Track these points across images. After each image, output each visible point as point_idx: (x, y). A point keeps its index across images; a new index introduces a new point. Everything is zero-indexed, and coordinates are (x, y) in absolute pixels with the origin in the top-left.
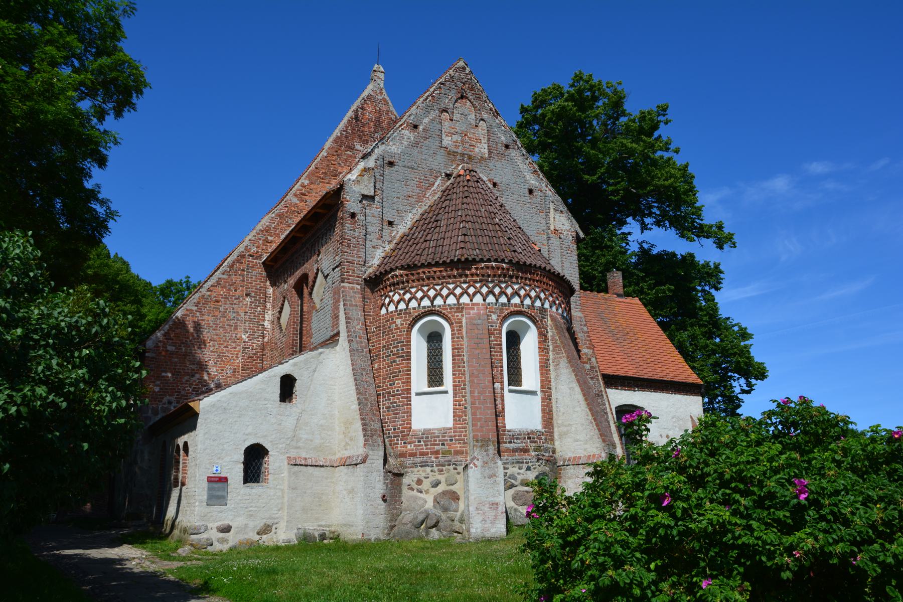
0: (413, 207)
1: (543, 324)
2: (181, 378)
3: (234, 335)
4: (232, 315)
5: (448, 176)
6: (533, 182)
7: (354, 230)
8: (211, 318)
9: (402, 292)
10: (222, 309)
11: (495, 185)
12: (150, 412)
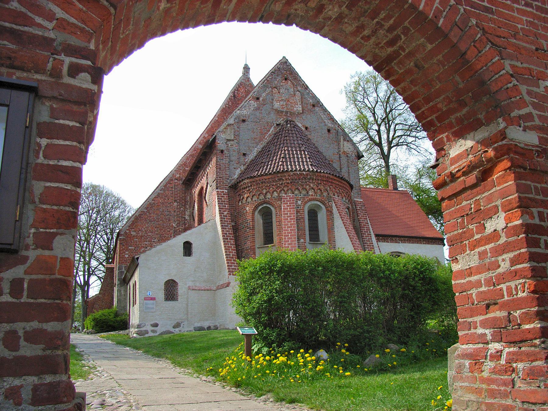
0: (258, 145)
1: (329, 205)
2: (140, 249)
3: (168, 224)
4: (167, 213)
5: (277, 125)
6: (330, 125)
7: (223, 160)
8: (155, 216)
10: (161, 210)
11: (306, 128)
12: (123, 269)
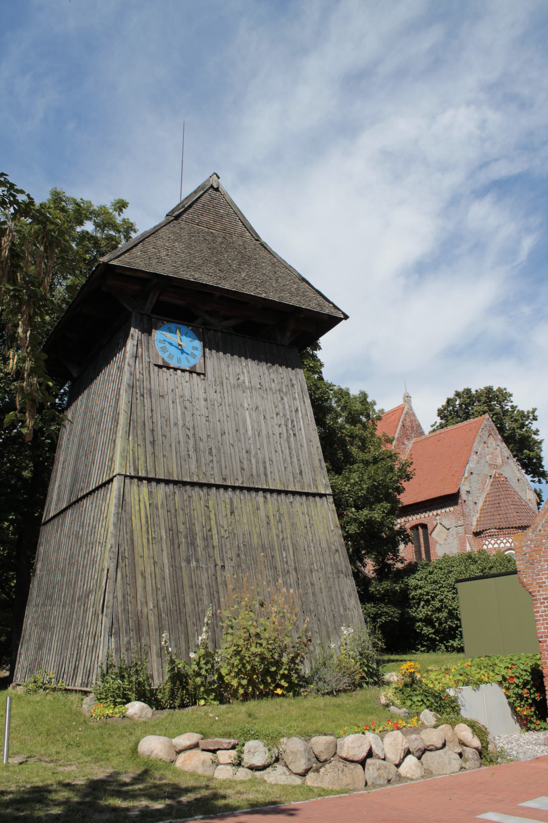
9: (496, 539)
